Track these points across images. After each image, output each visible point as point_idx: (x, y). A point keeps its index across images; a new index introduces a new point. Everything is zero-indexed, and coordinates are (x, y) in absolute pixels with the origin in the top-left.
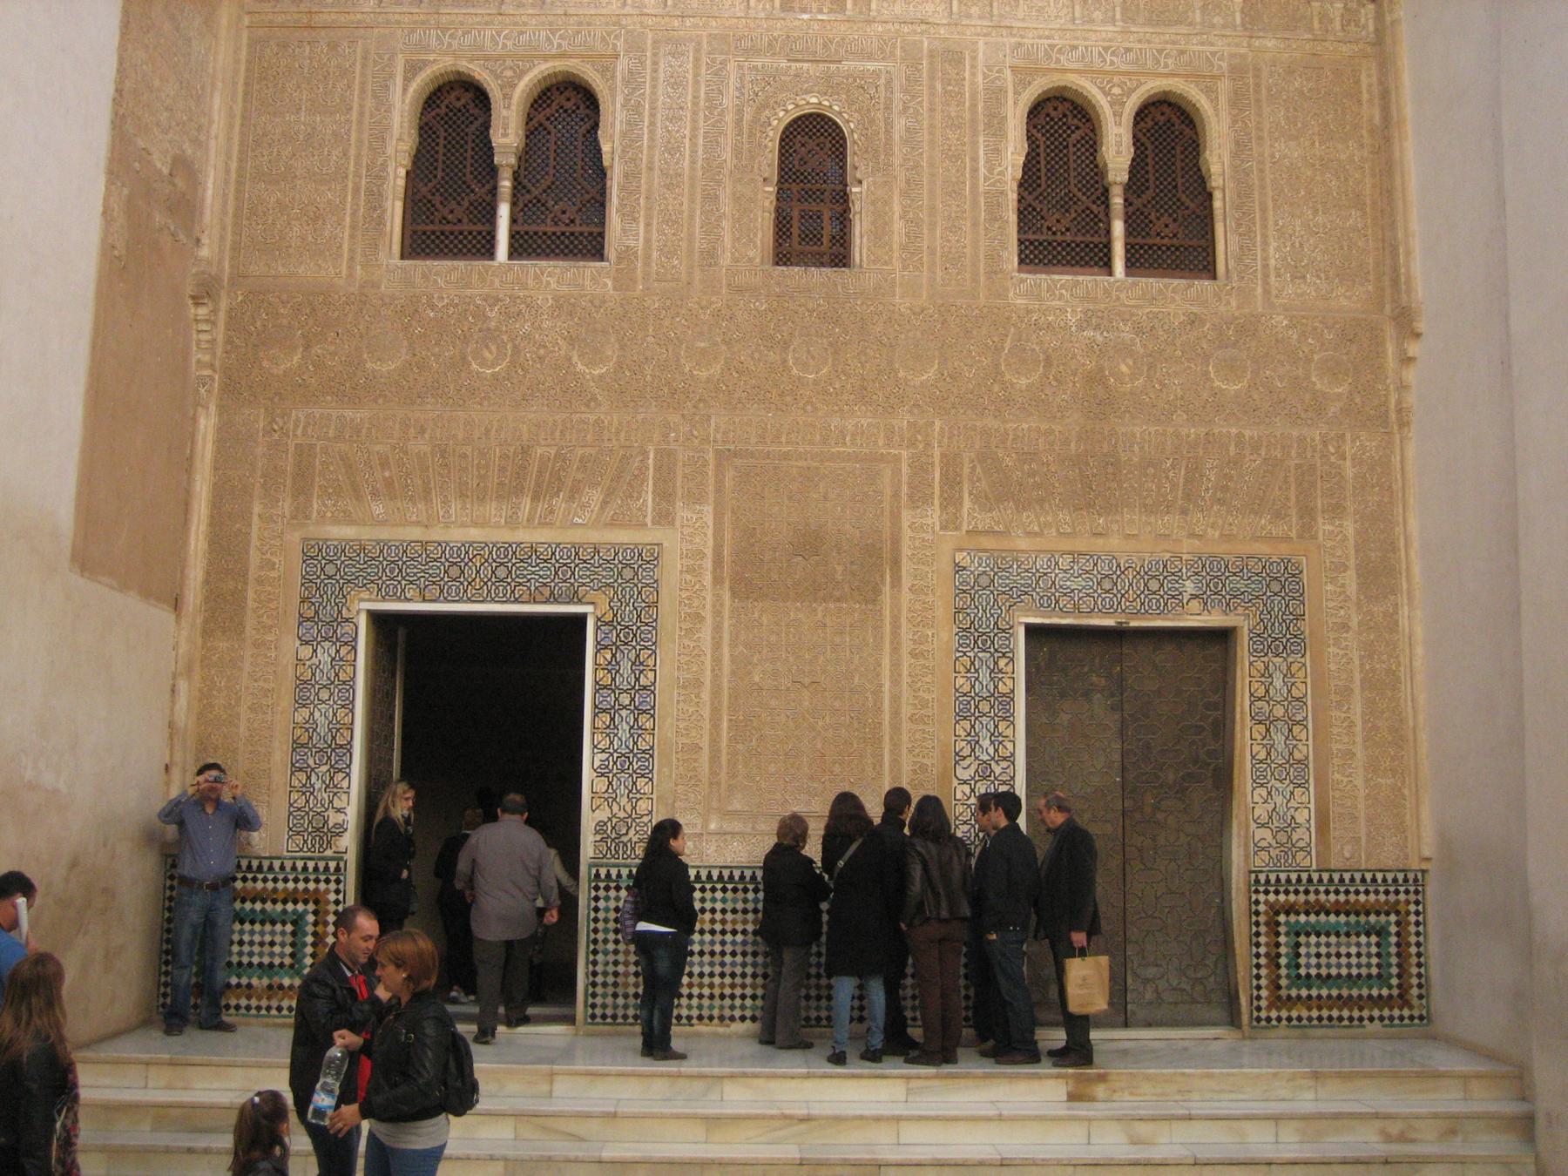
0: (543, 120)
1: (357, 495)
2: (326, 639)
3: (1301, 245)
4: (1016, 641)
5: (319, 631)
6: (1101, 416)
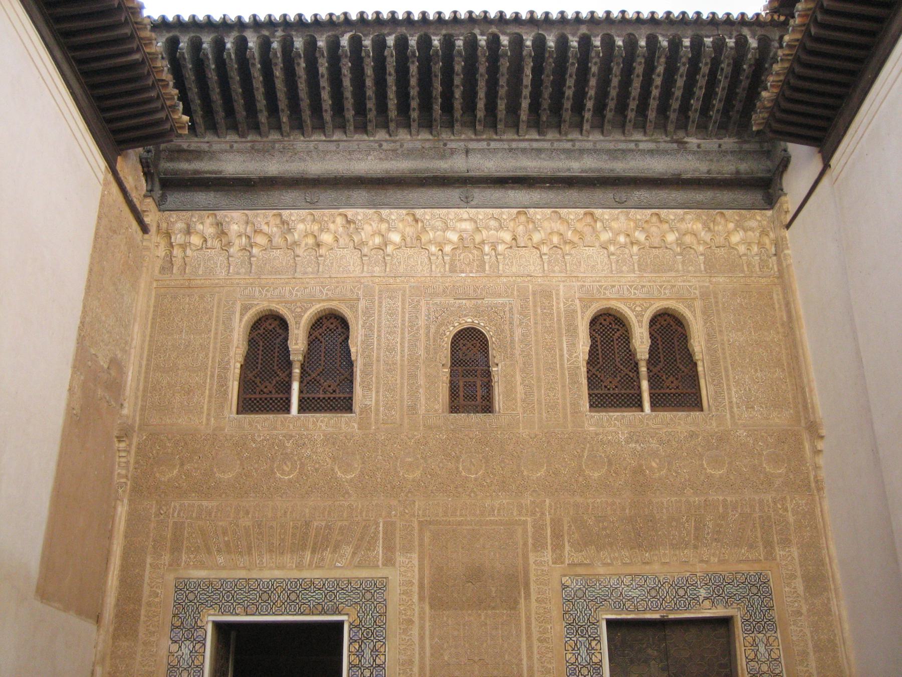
0: (318, 335)
1: (209, 551)
2: (188, 639)
3: (749, 389)
4: (601, 629)
5: (183, 634)
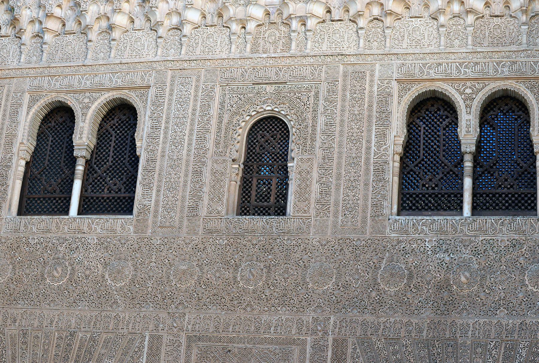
6: (446, 312)
